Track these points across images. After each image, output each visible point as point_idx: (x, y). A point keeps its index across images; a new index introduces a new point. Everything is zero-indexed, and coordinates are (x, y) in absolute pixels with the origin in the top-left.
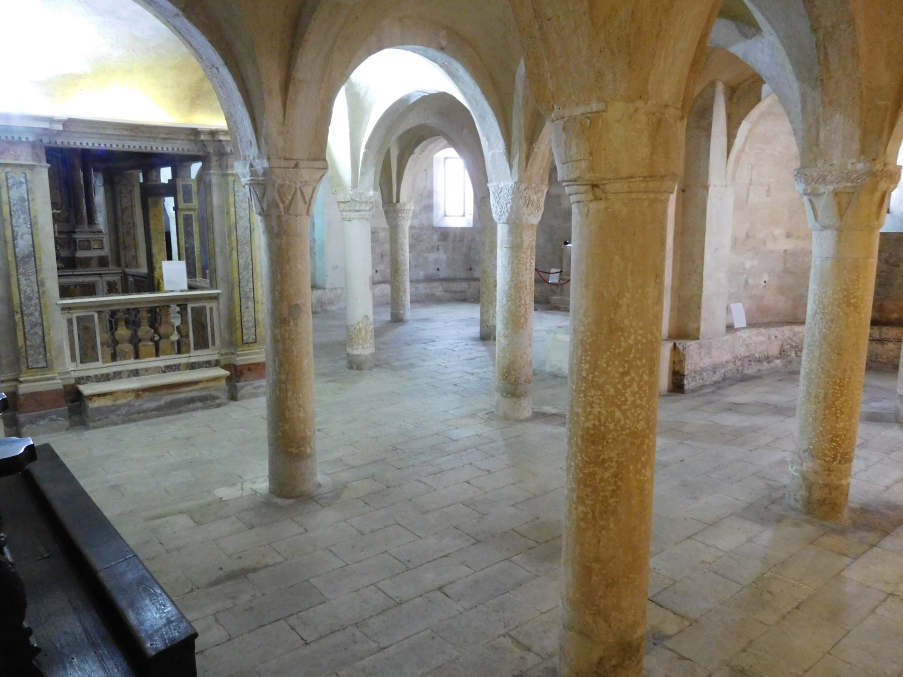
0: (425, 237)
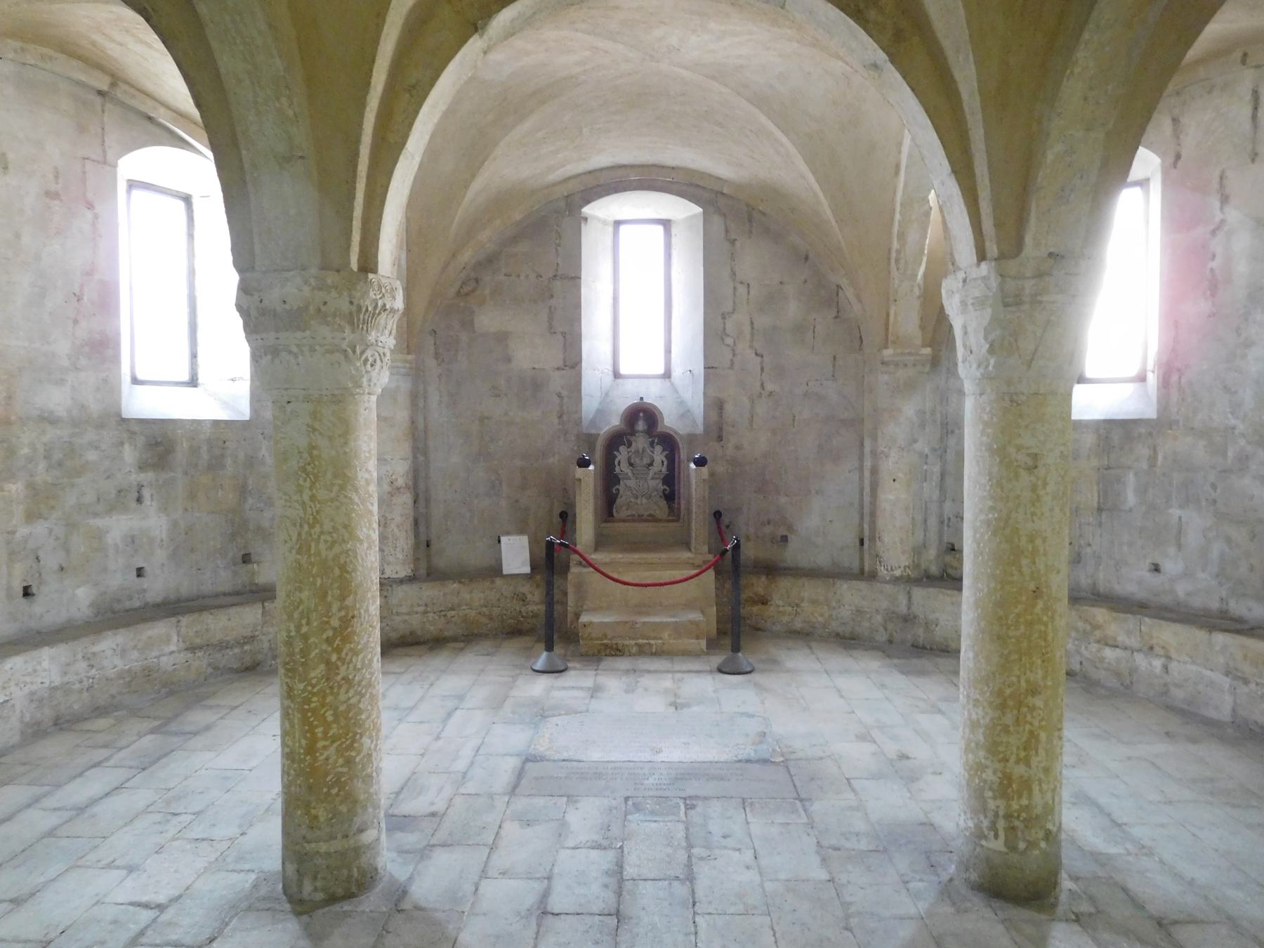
0: (92, 456)
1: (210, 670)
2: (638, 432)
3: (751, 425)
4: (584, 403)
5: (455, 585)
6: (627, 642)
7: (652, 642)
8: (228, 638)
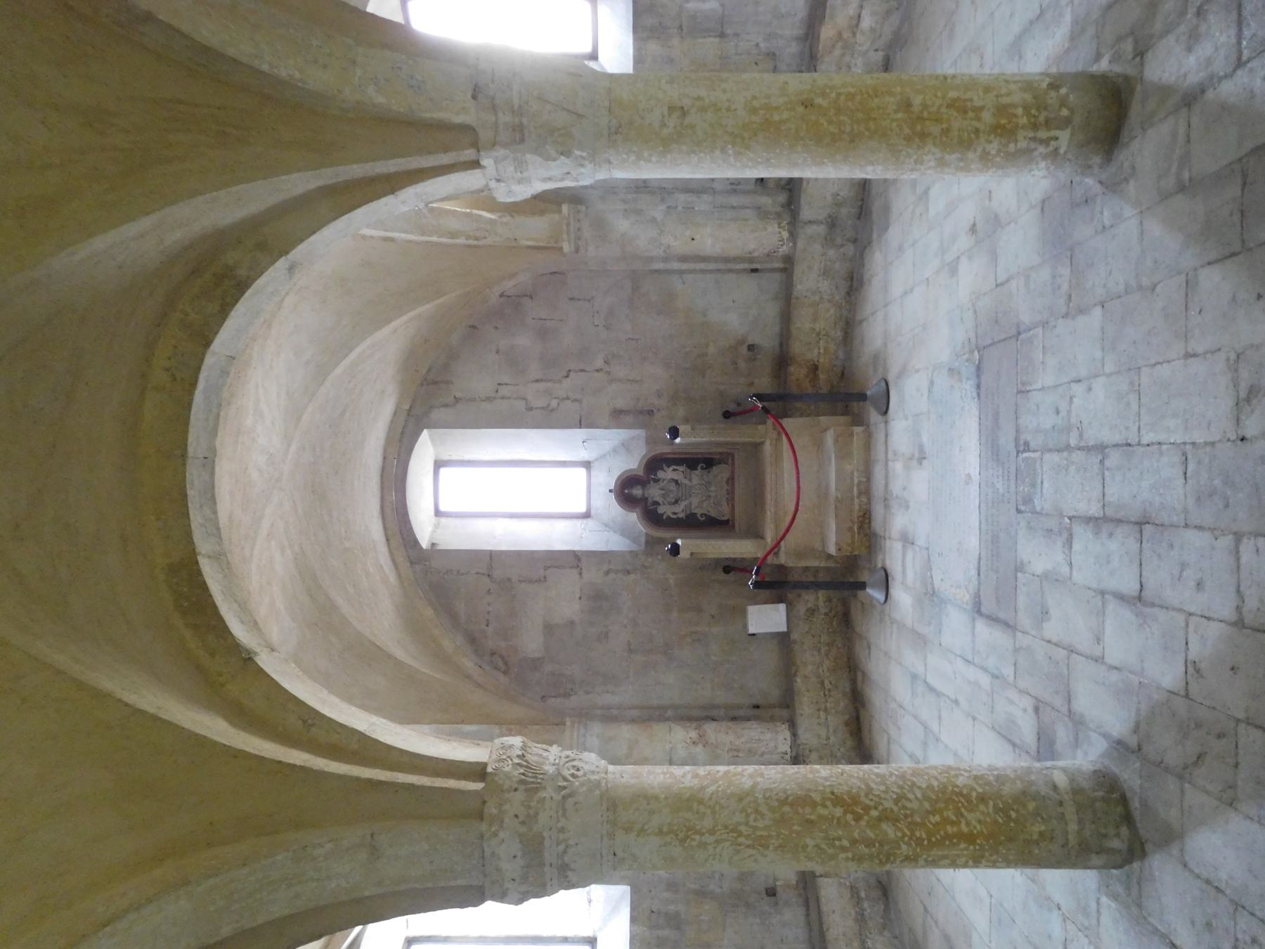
1: (886, 933)
2: (643, 494)
3: (636, 382)
4: (615, 548)
5: (798, 680)
6: (857, 507)
7: (856, 481)
8: (853, 912)
